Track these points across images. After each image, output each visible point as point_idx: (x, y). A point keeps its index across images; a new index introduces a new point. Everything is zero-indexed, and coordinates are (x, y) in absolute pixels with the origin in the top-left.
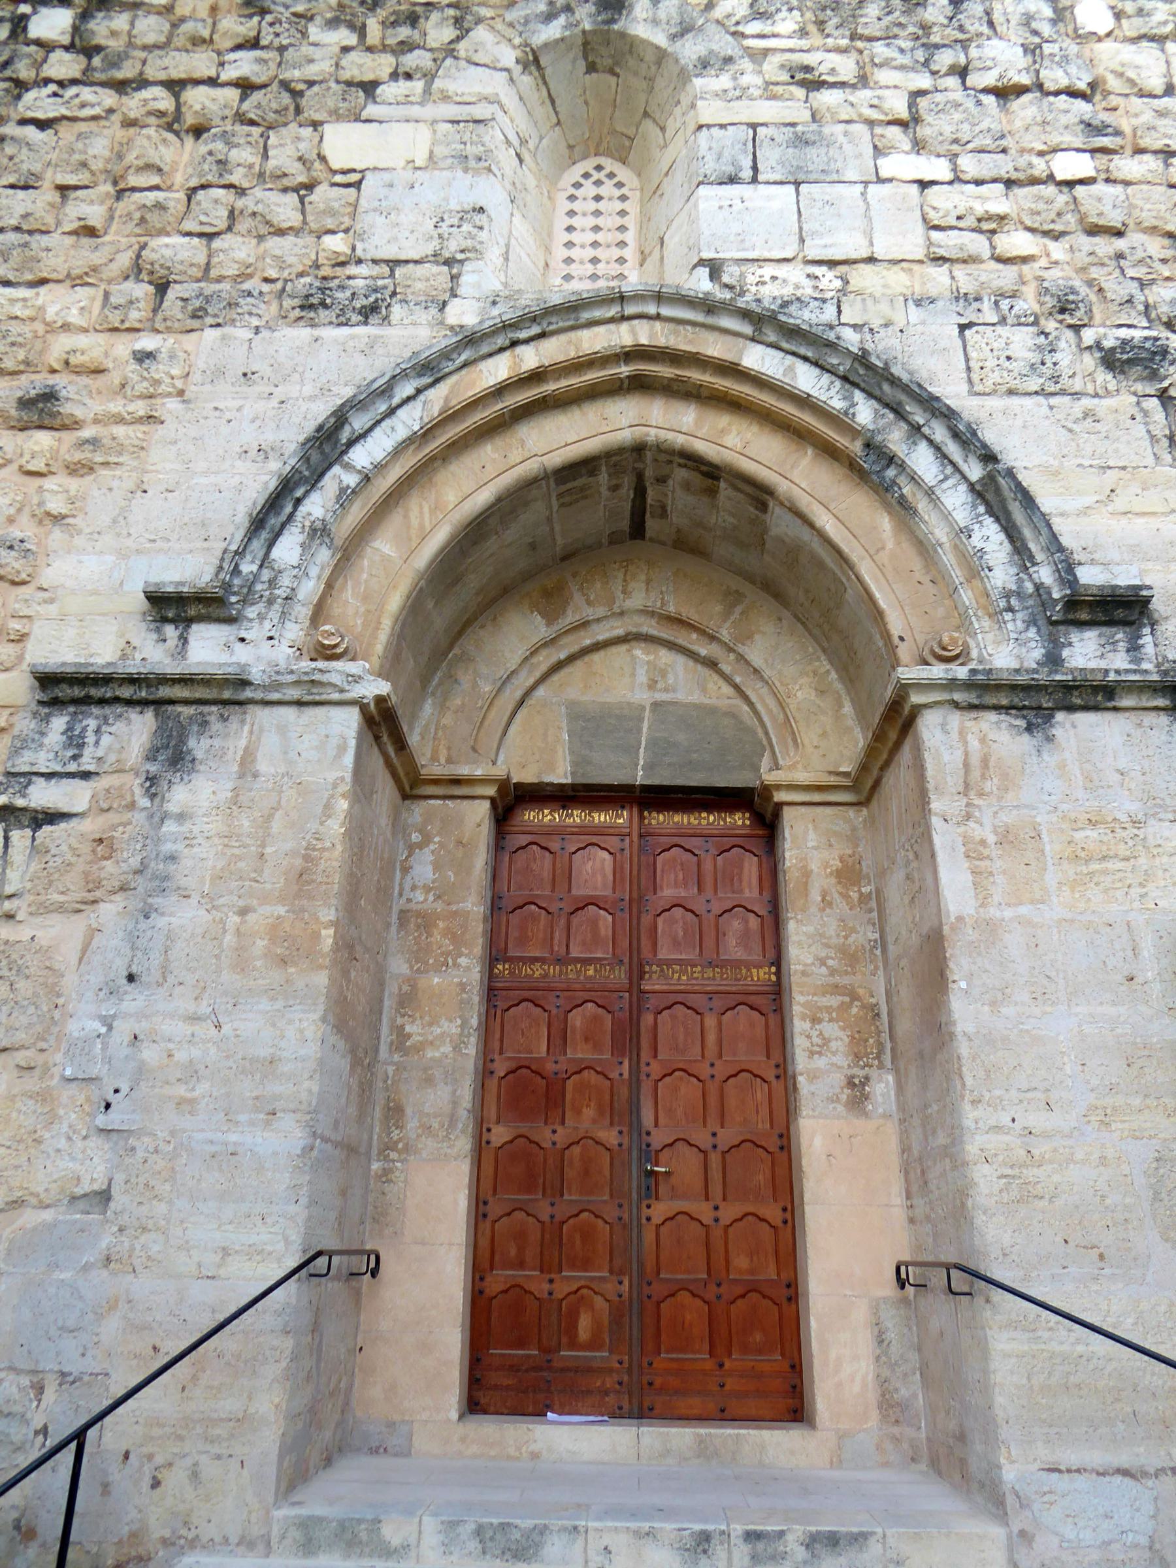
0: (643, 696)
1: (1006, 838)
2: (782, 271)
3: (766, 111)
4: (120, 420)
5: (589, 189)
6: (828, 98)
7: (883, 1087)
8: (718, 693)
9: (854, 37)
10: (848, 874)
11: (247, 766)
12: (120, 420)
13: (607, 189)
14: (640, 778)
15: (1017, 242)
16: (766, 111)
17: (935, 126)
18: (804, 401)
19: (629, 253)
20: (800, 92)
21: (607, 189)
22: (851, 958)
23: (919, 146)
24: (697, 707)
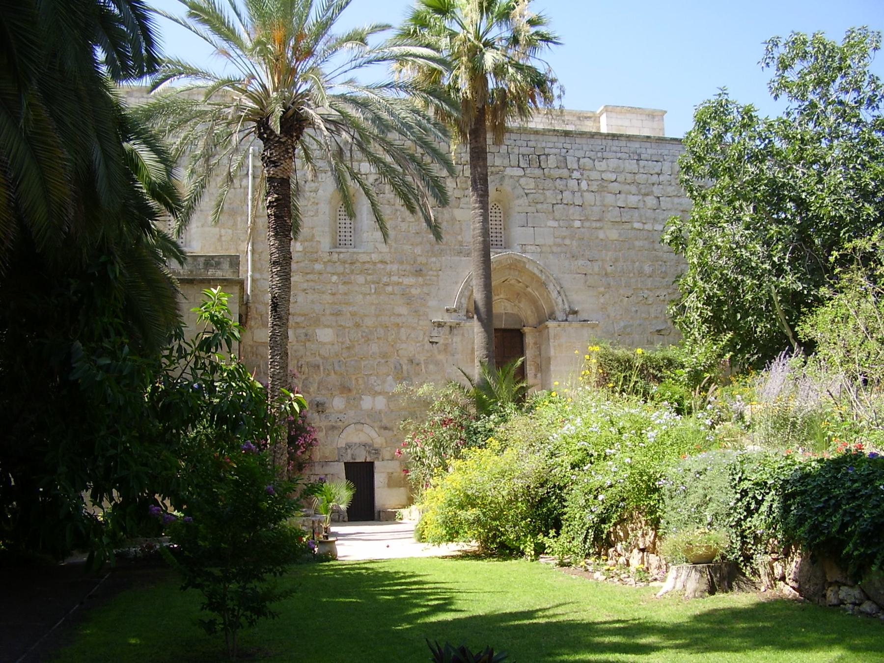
0: (503, 312)
1: (559, 345)
2: (532, 247)
3: (530, 209)
4: (432, 275)
5: (494, 210)
6: (539, 206)
7: (539, 375)
8: (515, 311)
9: (544, 189)
10: (535, 343)
11: (463, 335)
12: (432, 275)
13: (497, 210)
14: (503, 327)
15: (567, 242)
16: (530, 209)
17: (557, 214)
18: (534, 274)
19: (502, 227)
20: (533, 204)
21: (497, 210)
22: (536, 356)
23: (554, 219)
24: (512, 314)
